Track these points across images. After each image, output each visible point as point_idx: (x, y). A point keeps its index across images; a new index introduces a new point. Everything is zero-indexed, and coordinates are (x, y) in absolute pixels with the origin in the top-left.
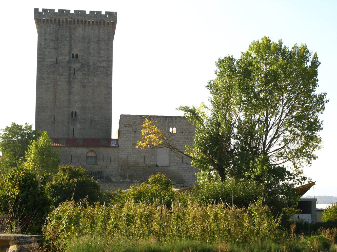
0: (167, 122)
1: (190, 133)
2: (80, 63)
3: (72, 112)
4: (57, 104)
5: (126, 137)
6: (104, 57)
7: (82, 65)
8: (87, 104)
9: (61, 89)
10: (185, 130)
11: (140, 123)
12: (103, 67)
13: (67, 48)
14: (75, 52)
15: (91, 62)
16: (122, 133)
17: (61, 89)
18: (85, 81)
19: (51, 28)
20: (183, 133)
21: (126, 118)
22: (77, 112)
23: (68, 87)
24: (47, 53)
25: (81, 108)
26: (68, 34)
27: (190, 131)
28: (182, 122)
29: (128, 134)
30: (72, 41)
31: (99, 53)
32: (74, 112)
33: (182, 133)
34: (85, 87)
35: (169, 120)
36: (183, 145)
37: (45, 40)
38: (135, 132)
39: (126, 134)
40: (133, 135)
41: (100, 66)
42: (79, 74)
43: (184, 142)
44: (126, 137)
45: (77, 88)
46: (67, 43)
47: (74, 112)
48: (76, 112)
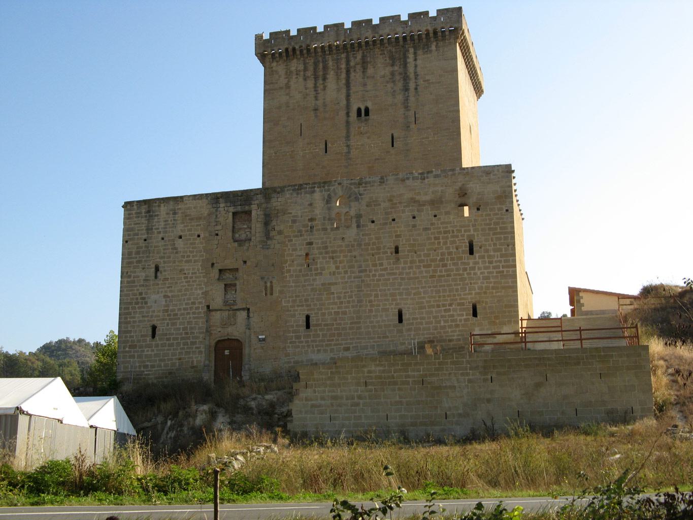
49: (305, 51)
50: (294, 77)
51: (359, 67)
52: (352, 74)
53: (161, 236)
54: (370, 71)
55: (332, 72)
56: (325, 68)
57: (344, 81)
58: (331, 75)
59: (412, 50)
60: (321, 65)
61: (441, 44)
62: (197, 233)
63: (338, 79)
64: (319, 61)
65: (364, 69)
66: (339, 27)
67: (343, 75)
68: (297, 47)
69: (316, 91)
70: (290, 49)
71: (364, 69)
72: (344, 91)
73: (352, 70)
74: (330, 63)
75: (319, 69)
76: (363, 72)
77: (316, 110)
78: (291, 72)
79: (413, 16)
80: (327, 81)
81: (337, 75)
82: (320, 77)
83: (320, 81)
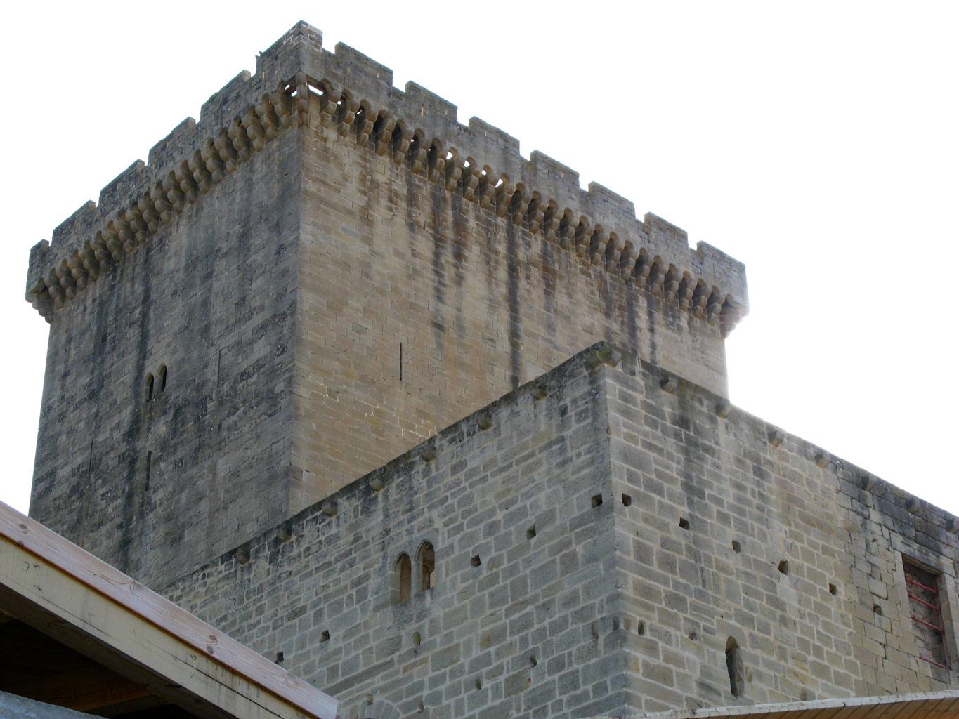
0: (379, 517)
1: (532, 533)
2: (170, 408)
6: (262, 308)
7: (178, 411)
10: (492, 529)
11: (225, 618)
12: (258, 366)
13: (132, 358)
14: (152, 368)
15: (211, 374)
19: (89, 302)
20: (484, 561)
24: (64, 438)
26: (139, 288)
27: (531, 520)
28: (471, 465)
31: (243, 300)
33: (476, 561)
34: (181, 538)
35: (386, 497)
36: (484, 670)
37: (65, 375)
41: (244, 375)
43: (488, 640)
46: (133, 333)
49: (423, 152)
50: (384, 202)
51: (536, 273)
52: (522, 284)
53: (732, 533)
54: (561, 299)
55: (476, 249)
56: (459, 225)
57: (503, 290)
58: (474, 253)
59: (643, 303)
60: (449, 214)
61: (697, 323)
62: (830, 577)
63: (490, 276)
64: (444, 199)
65: (548, 285)
66: (508, 144)
67: (502, 274)
68: (411, 128)
69: (437, 273)
70: (390, 123)
71: (549, 290)
72: (504, 314)
73: (521, 273)
74: (472, 224)
75: (445, 220)
76: (547, 293)
77: (439, 326)
78: (375, 185)
79: (655, 224)
80: (464, 263)
81: (488, 263)
82: (449, 245)
83: (448, 257)
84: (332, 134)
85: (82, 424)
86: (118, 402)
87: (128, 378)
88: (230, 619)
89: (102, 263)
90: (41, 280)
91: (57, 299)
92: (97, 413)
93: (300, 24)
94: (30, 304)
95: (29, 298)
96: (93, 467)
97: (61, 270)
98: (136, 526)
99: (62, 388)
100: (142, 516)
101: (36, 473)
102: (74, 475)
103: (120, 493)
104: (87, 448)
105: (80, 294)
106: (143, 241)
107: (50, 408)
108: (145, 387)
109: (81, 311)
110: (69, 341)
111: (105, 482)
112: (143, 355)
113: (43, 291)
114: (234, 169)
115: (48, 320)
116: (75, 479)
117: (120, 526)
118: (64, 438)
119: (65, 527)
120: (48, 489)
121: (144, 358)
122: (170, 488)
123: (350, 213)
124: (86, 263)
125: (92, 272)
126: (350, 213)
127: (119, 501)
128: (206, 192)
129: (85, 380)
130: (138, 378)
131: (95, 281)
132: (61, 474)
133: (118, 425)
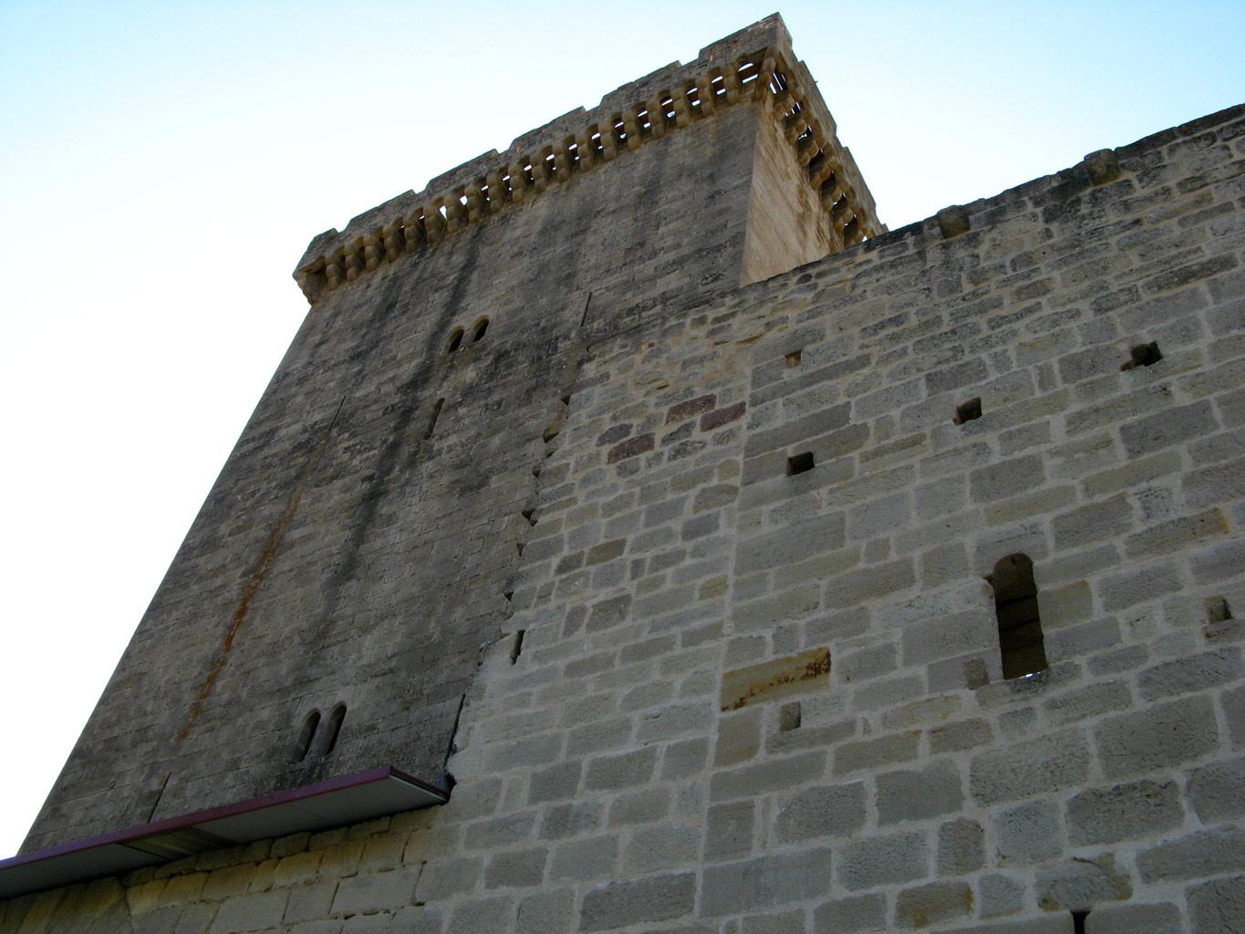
3: (315, 718)
4: (219, 685)
5: (617, 607)
8: (459, 612)
9: (291, 571)
14: (465, 321)
16: (555, 561)
17: (291, 571)
18: (496, 441)
21: (655, 354)
22: (349, 709)
23: (348, 534)
25: (393, 663)
29: (669, 535)
30: (475, 276)
32: (325, 717)
38: (802, 464)
39: (627, 556)
40: (767, 529)
42: (458, 420)
44: (617, 607)
45: (416, 509)
46: (440, 298)
47: (325, 717)
48: (341, 710)
84: (781, 134)
85: (332, 384)
86: (399, 357)
87: (429, 321)
88: (913, 321)
89: (410, 242)
90: (323, 257)
91: (333, 280)
92: (360, 372)
93: (777, 14)
94: (295, 283)
95: (295, 276)
96: (341, 421)
97: (352, 246)
98: (398, 478)
99: (312, 355)
100: (412, 463)
101: (244, 434)
102: (305, 431)
103: (378, 444)
104: (336, 403)
105: (365, 276)
106: (476, 220)
107: (287, 375)
108: (445, 341)
109: (365, 291)
110: (336, 315)
111: (353, 435)
112: (452, 308)
113: (316, 273)
114: (637, 147)
115: (311, 301)
116: (307, 436)
117: (370, 478)
118: (300, 399)
119: (274, 484)
120: (260, 448)
121: (453, 314)
122: (473, 433)
123: (792, 210)
124: (389, 240)
125: (391, 252)
126: (792, 210)
127: (376, 452)
128: (587, 169)
129: (350, 344)
130: (442, 326)
131: (391, 262)
132: (283, 432)
133: (392, 379)
